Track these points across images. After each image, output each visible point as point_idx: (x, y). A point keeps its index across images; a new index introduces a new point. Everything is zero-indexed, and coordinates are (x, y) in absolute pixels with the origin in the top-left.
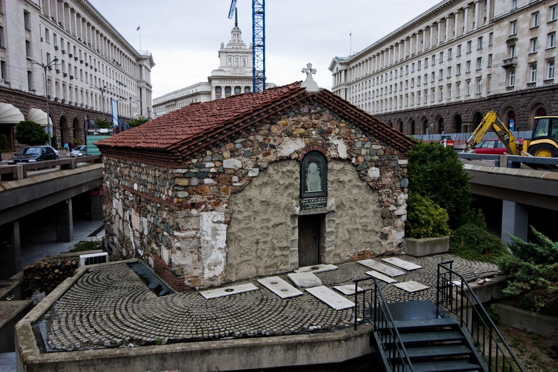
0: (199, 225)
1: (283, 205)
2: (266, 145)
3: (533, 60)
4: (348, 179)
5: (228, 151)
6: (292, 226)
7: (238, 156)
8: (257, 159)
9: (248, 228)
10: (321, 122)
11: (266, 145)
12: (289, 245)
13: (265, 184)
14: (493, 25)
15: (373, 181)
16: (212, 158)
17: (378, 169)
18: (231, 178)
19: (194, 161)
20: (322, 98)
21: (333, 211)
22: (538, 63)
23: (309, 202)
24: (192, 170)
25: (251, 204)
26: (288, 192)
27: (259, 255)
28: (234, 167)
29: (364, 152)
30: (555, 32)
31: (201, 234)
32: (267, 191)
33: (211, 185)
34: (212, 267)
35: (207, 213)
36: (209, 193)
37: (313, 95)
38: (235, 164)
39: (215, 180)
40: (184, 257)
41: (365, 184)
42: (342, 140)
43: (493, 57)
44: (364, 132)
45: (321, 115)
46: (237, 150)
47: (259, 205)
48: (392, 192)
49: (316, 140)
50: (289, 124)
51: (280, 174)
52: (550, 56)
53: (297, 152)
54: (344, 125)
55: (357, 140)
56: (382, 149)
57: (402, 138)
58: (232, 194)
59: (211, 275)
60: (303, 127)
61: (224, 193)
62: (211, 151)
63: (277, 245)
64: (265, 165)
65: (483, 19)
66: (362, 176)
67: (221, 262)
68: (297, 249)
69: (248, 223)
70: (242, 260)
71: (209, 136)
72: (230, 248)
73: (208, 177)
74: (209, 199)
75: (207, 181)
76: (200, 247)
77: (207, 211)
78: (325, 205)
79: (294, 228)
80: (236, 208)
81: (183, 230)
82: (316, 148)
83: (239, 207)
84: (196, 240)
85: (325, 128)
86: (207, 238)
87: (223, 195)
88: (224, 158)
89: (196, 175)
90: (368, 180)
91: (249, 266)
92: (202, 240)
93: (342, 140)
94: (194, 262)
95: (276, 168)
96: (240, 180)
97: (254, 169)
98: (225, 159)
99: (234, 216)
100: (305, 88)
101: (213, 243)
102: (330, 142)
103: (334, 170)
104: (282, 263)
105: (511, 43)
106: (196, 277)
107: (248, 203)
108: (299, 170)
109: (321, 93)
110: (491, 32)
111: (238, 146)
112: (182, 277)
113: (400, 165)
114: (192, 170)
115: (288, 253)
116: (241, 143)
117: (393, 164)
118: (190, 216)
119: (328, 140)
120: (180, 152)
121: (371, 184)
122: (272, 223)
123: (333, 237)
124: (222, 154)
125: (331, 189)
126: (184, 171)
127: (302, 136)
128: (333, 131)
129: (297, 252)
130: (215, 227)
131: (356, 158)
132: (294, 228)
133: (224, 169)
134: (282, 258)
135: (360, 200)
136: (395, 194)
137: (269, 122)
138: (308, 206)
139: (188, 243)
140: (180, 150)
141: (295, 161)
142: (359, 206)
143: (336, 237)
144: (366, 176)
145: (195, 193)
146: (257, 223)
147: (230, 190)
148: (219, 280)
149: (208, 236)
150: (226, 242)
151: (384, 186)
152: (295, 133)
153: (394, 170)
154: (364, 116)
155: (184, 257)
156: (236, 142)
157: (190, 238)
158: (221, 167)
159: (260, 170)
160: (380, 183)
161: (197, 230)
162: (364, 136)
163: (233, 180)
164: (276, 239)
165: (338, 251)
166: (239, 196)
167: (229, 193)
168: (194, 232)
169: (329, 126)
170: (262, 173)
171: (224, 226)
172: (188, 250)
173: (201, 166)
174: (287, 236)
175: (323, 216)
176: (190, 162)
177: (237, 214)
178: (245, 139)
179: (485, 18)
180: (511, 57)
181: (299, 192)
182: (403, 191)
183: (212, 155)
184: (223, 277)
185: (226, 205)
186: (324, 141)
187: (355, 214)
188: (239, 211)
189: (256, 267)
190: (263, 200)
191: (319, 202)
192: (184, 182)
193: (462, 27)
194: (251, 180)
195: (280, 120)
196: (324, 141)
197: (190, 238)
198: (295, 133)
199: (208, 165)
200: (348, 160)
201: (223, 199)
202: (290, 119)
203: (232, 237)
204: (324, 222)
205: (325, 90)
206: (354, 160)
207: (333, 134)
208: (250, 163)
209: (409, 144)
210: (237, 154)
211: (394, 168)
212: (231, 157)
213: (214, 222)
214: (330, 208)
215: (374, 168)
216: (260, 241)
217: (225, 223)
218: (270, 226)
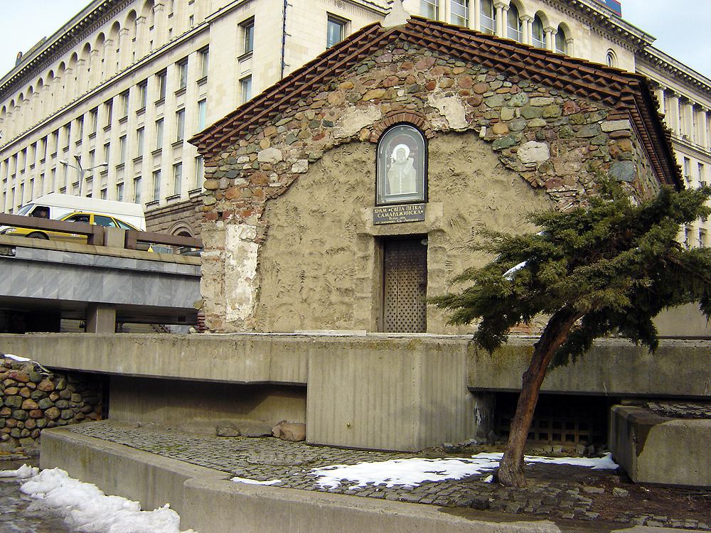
1: (345, 218)
2: (318, 123)
4: (475, 169)
5: (268, 139)
6: (360, 254)
8: (305, 145)
9: (290, 253)
11: (318, 123)
12: (354, 286)
13: (317, 183)
15: (533, 170)
17: (543, 145)
19: (225, 155)
20: (412, 33)
21: (441, 231)
24: (222, 169)
29: (506, 113)
32: (322, 195)
34: (237, 305)
37: (397, 33)
38: (272, 156)
40: (206, 286)
42: (454, 97)
44: (508, 75)
47: (307, 215)
51: (342, 166)
53: (370, 128)
54: (461, 70)
55: (492, 94)
57: (599, 73)
59: (236, 317)
60: (381, 86)
63: (333, 283)
64: (316, 155)
67: (249, 299)
70: (280, 303)
71: (235, 118)
74: (239, 206)
75: (238, 181)
76: (224, 274)
79: (365, 258)
81: (207, 248)
82: (403, 118)
84: (220, 264)
85: (422, 82)
86: (233, 262)
90: (520, 168)
91: (291, 314)
97: (300, 161)
99: (271, 232)
101: (239, 269)
107: (292, 214)
109: (410, 26)
111: (281, 129)
114: (222, 169)
117: (586, 131)
122: (327, 247)
127: (377, 101)
128: (438, 85)
129: (371, 300)
132: (365, 258)
134: (344, 308)
135: (503, 211)
137: (327, 88)
138: (387, 219)
139: (211, 266)
141: (368, 144)
144: (513, 160)
151: (560, 179)
152: (366, 98)
154: (497, 44)
156: (277, 124)
157: (214, 260)
158: (256, 162)
159: (309, 163)
160: (551, 172)
162: (508, 84)
163: (272, 179)
166: (280, 202)
167: (264, 197)
168: (218, 253)
170: (314, 167)
171: (255, 247)
178: (291, 119)
190: (314, 208)
191: (410, 213)
194: (295, 179)
196: (420, 103)
199: (241, 160)
202: (358, 78)
205: (412, 17)
206: (483, 133)
207: (437, 89)
208: (294, 152)
210: (276, 140)
212: (271, 146)
218: (324, 252)
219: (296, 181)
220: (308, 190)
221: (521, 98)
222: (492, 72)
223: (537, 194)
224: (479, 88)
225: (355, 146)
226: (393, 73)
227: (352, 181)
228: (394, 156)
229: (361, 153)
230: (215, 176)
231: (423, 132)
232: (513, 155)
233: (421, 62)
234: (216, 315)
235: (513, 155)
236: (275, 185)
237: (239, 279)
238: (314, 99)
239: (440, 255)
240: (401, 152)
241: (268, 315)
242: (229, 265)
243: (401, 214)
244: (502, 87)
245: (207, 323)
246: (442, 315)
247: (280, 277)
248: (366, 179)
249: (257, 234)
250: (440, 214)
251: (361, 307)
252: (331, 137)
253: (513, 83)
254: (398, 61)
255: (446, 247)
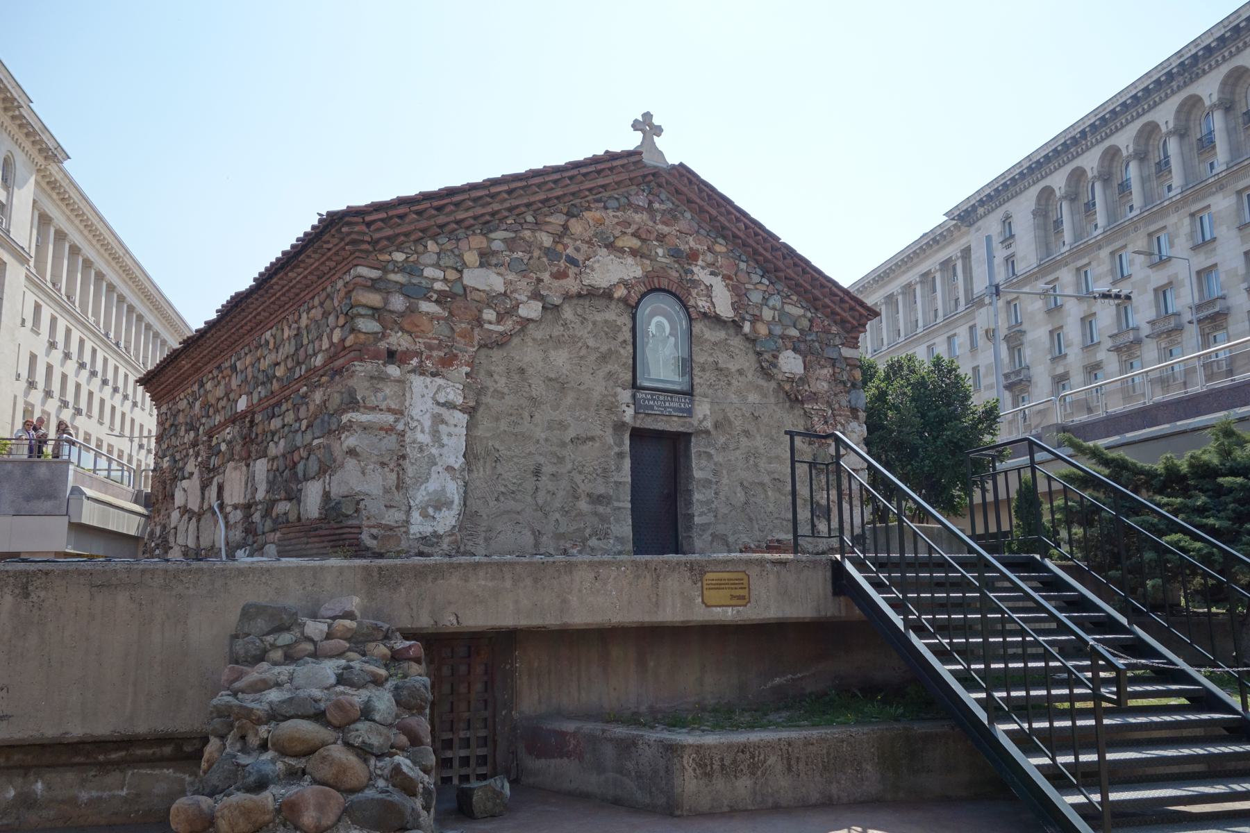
0: (402, 403)
1: (596, 396)
2: (558, 256)
3: (1060, 370)
4: (738, 367)
5: (475, 252)
6: (616, 449)
7: (496, 265)
8: (539, 280)
10: (674, 232)
11: (558, 256)
14: (973, 311)
15: (790, 380)
16: (439, 258)
18: (480, 311)
19: (399, 257)
20: (675, 182)
21: (707, 432)
22: (1071, 373)
23: (654, 400)
24: (392, 277)
25: (524, 380)
26: (607, 370)
27: (540, 502)
28: (487, 288)
30: (1095, 313)
31: (407, 424)
32: (561, 359)
33: (433, 318)
34: (431, 511)
35: (422, 378)
36: (430, 335)
39: (444, 309)
40: (363, 473)
41: (773, 384)
42: (720, 278)
43: (982, 371)
45: (675, 218)
46: (494, 253)
47: (543, 386)
48: (834, 415)
49: (664, 268)
50: (607, 222)
52: (1092, 360)
55: (751, 287)
56: (804, 316)
57: (847, 298)
58: (481, 347)
59: (428, 529)
60: (635, 235)
61: (463, 341)
62: (437, 244)
63: (582, 486)
65: (953, 303)
66: (767, 370)
67: (452, 502)
68: (629, 506)
69: (516, 424)
72: (475, 475)
73: (429, 299)
74: (430, 347)
75: (426, 306)
76: (404, 457)
77: (422, 374)
78: (690, 412)
79: (620, 455)
80: (489, 382)
81: (366, 408)
82: (664, 284)
83: (496, 383)
86: (423, 438)
87: (461, 346)
88: (465, 265)
89: (402, 289)
90: (780, 377)
92: (408, 440)
93: (720, 278)
94: (387, 491)
95: (579, 311)
96: (499, 320)
98: (467, 267)
99: (484, 399)
100: (640, 153)
101: (434, 451)
102: (696, 277)
103: (706, 340)
104: (594, 533)
105: (1015, 340)
106: (391, 529)
107: (516, 377)
108: (630, 325)
109: (675, 172)
110: (971, 324)
112: (355, 522)
113: (846, 359)
114: (392, 277)
115: (608, 510)
116: (505, 240)
118: (383, 378)
119: (692, 272)
120: (369, 224)
121: (787, 387)
122: (571, 433)
123: (710, 494)
124: (460, 256)
125: (701, 381)
126: (375, 274)
127: (634, 253)
128: (701, 257)
130: (440, 415)
131: (753, 323)
132: (620, 455)
133: (465, 288)
136: (838, 418)
137: (565, 210)
138: (652, 408)
139: (376, 440)
140: (368, 218)
141: (621, 304)
142: (763, 431)
143: (716, 493)
145: (396, 329)
146: (536, 425)
147: (477, 338)
148: (445, 546)
149: (423, 431)
150: (464, 456)
151: (814, 397)
153: (834, 366)
154: (766, 236)
155: (363, 473)
156: (492, 235)
157: (381, 429)
160: (806, 387)
161: (399, 413)
162: (765, 281)
164: (580, 473)
165: (720, 529)
166: (497, 354)
167: (475, 343)
168: (390, 418)
169: (692, 244)
170: (549, 316)
171: (462, 418)
172: (374, 459)
173: (412, 269)
174: (605, 470)
175: (686, 437)
176: (390, 258)
177: (492, 397)
178: (513, 235)
179: (957, 300)
180: (1018, 368)
181: (631, 374)
182: (856, 418)
183: (438, 254)
184: (456, 542)
185: (468, 369)
186: (683, 275)
187: (756, 448)
188: (495, 391)
189: (533, 533)
190: (553, 375)
191: (677, 405)
192: (374, 299)
193: (913, 319)
195: (589, 209)
196: (683, 275)
197: (381, 429)
198: (619, 243)
199: (429, 272)
200: (736, 325)
201: (460, 354)
203: (479, 449)
204: (688, 457)
205: (681, 165)
206: (747, 328)
207: (700, 263)
209: (861, 315)
210: (494, 261)
211: (833, 362)
212: (481, 265)
213: (438, 403)
214: (701, 422)
215: (790, 353)
216: (544, 469)
217: (463, 411)
219: (523, 329)
220: (542, 347)
221: (775, 301)
222: (752, 263)
223: (792, 407)
224: (742, 277)
225: (603, 302)
226: (651, 224)
227: (604, 349)
228: (652, 328)
229: (613, 314)
230: (382, 285)
231: (687, 309)
232: (775, 361)
233: (683, 225)
234: (386, 525)
235: (775, 361)
236: (492, 327)
237: (434, 468)
238: (548, 219)
239: (704, 463)
240: (659, 325)
241: (484, 529)
242: (414, 442)
243: (667, 404)
244: (760, 282)
245: (366, 539)
246: (711, 534)
247: (499, 470)
248: (622, 351)
249: (465, 398)
250: (708, 412)
251: (617, 521)
252: (578, 281)
253: (771, 283)
254: (657, 210)
255: (712, 452)
